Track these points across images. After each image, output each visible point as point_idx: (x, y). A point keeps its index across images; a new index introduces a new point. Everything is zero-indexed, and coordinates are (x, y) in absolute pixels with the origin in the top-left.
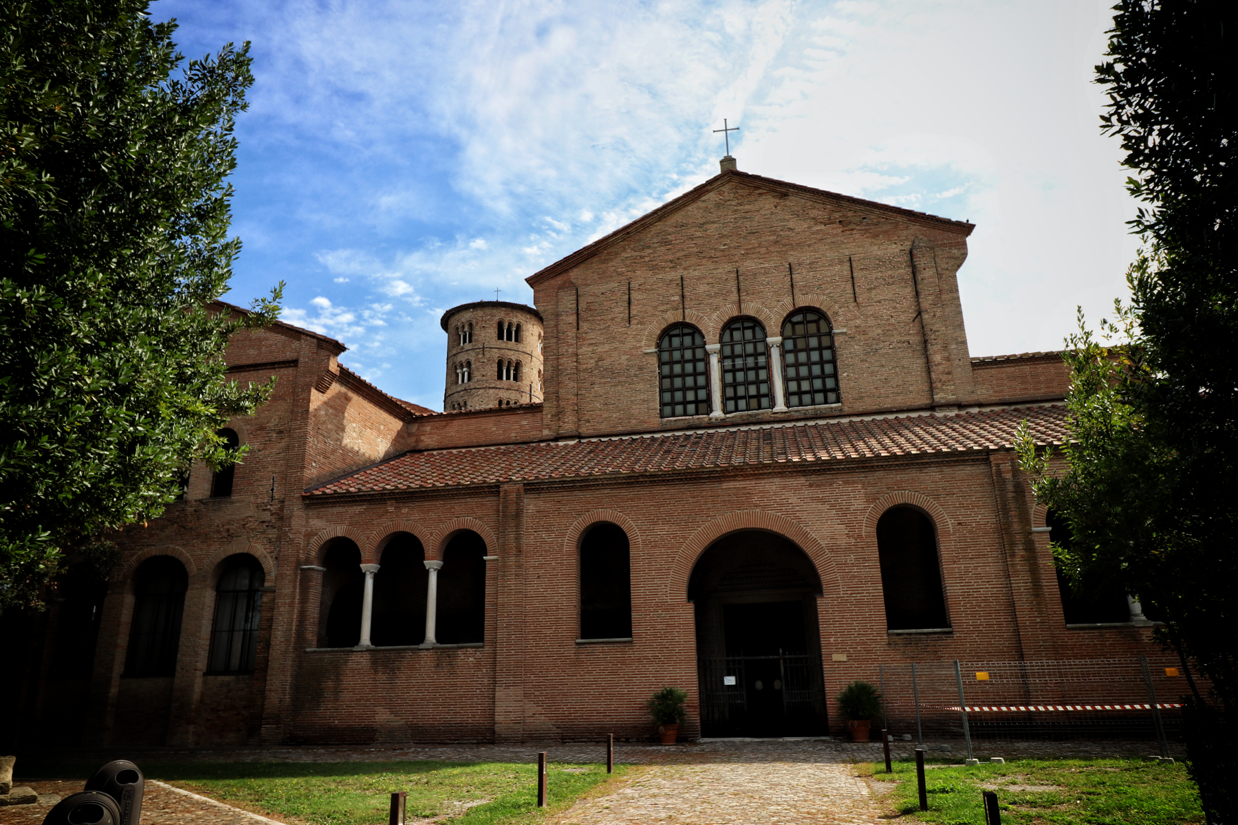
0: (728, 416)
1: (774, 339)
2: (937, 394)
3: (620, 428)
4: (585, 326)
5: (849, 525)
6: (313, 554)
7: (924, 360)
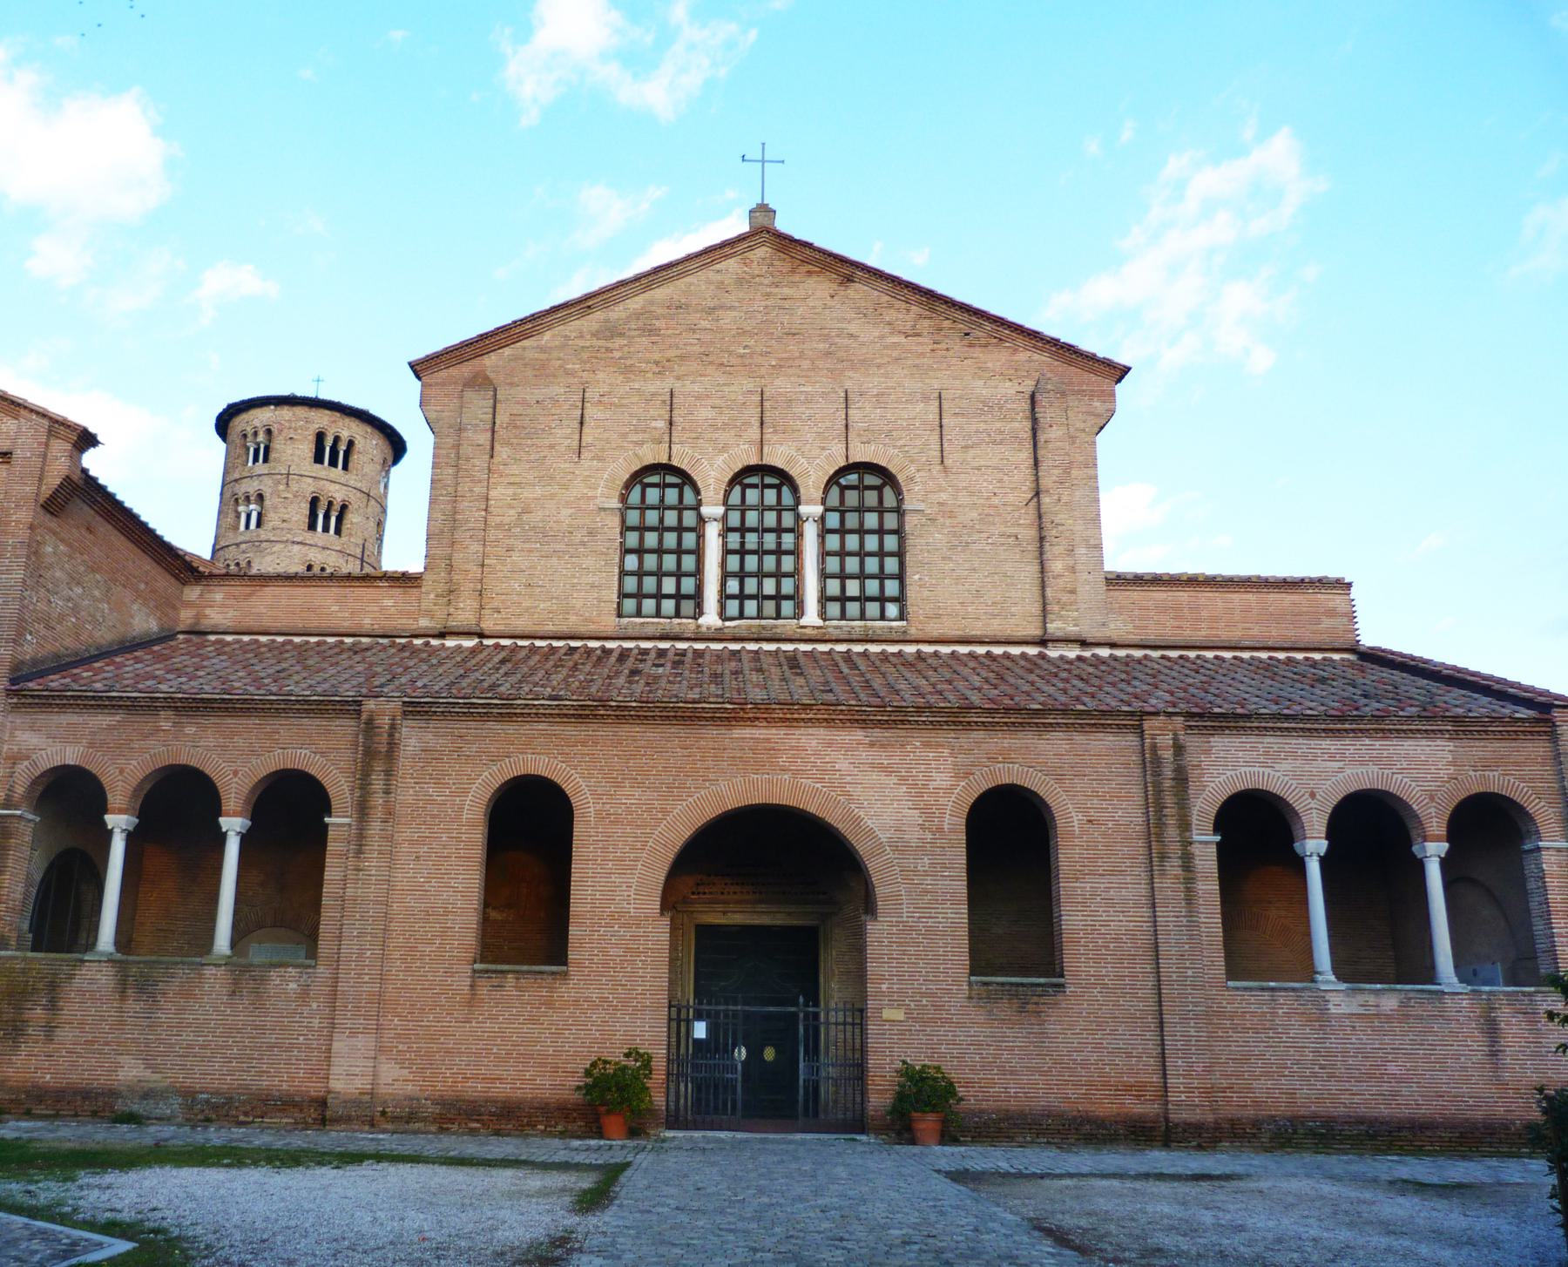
0: (728, 624)
1: (811, 509)
2: (1052, 621)
3: (550, 628)
4: (503, 452)
5: (926, 811)
6: (20, 790)
7: (1037, 568)
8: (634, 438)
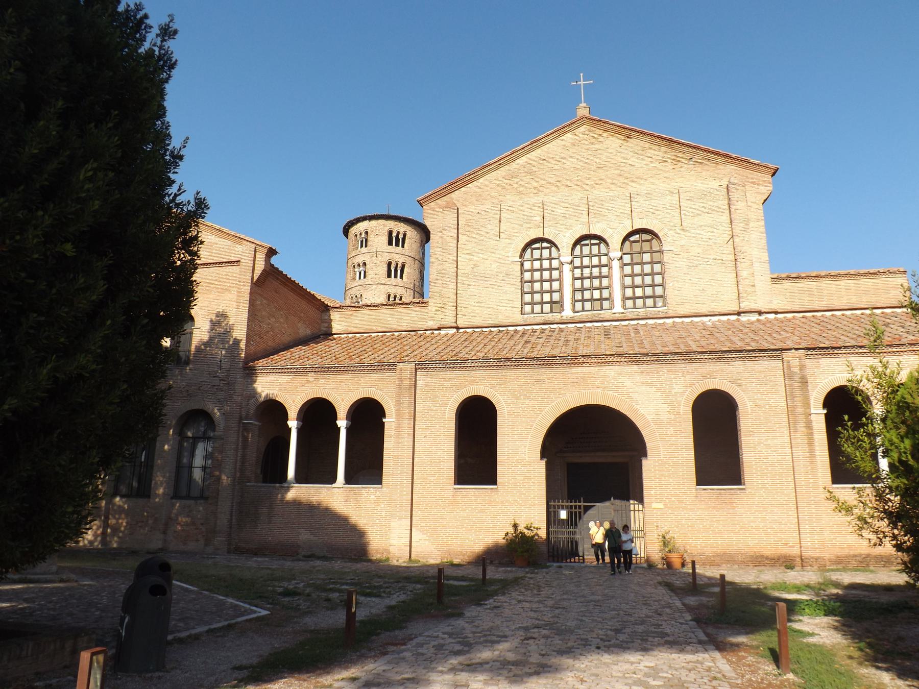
1: (615, 254)
3: (490, 322)
6: (252, 412)
8: (525, 226)
